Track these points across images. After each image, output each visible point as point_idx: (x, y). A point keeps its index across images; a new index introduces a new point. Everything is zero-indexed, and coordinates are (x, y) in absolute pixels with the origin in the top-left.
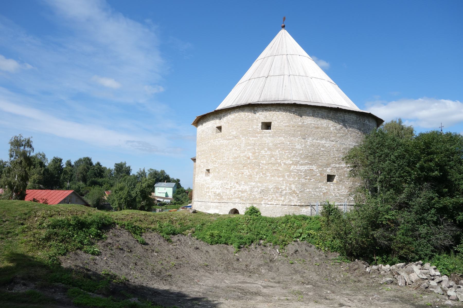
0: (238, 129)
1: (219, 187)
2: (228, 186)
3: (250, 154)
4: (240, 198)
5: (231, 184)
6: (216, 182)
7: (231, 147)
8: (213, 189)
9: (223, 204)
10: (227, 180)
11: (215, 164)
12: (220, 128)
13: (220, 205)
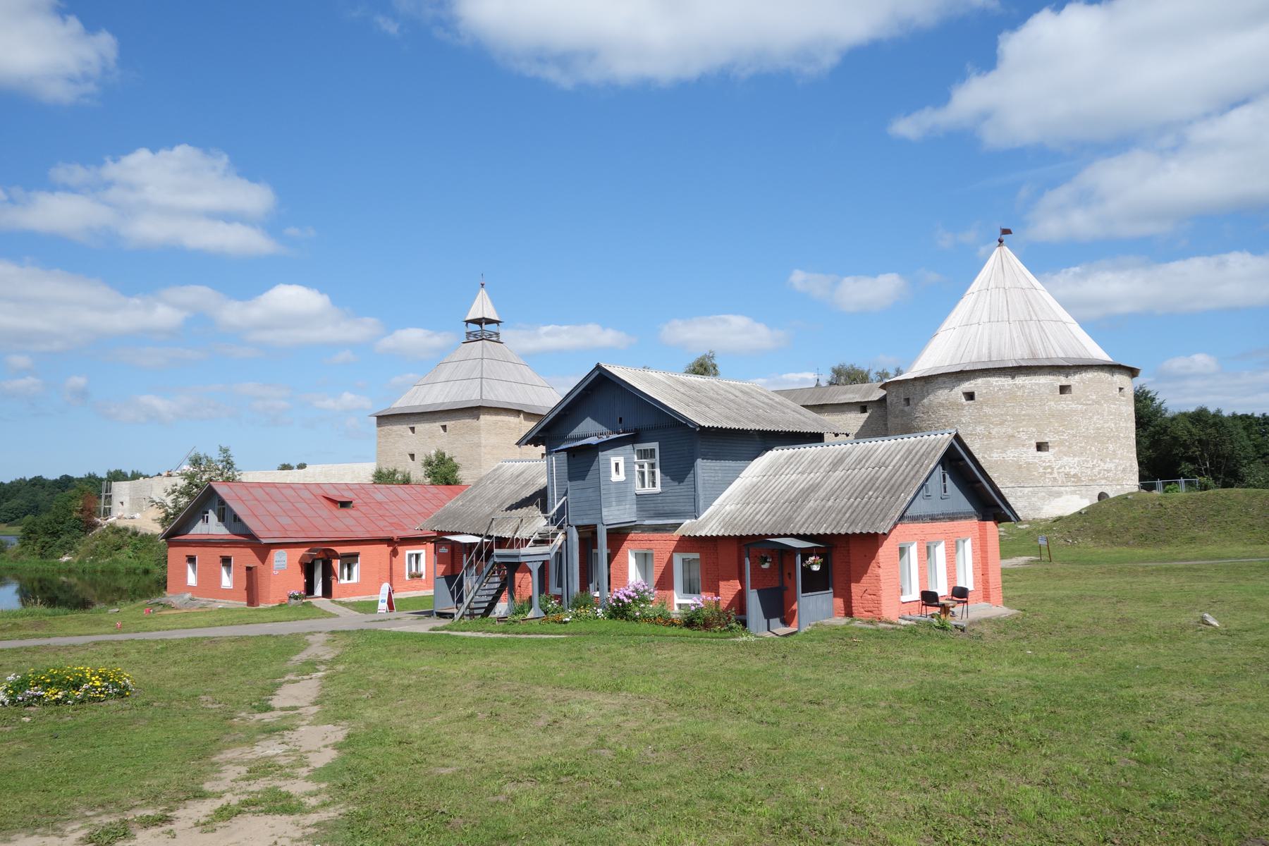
0: (1098, 392)
1: (1075, 465)
3: (1113, 425)
4: (1105, 478)
5: (1092, 462)
9: (1083, 488)
11: (1062, 435)
12: (1064, 389)
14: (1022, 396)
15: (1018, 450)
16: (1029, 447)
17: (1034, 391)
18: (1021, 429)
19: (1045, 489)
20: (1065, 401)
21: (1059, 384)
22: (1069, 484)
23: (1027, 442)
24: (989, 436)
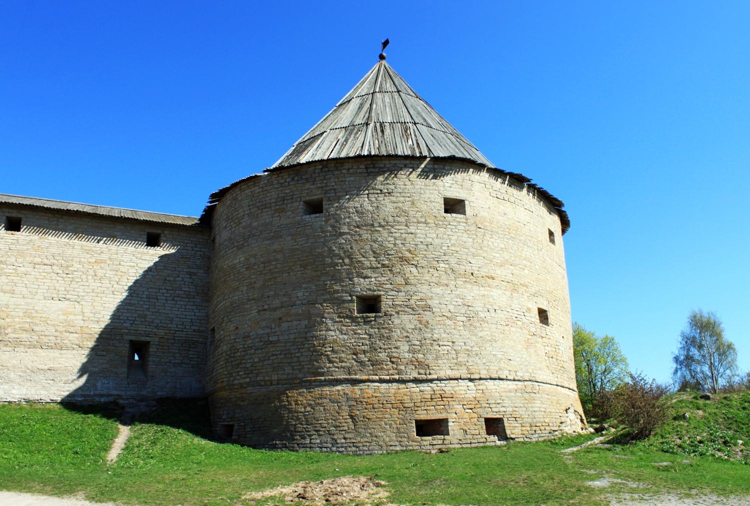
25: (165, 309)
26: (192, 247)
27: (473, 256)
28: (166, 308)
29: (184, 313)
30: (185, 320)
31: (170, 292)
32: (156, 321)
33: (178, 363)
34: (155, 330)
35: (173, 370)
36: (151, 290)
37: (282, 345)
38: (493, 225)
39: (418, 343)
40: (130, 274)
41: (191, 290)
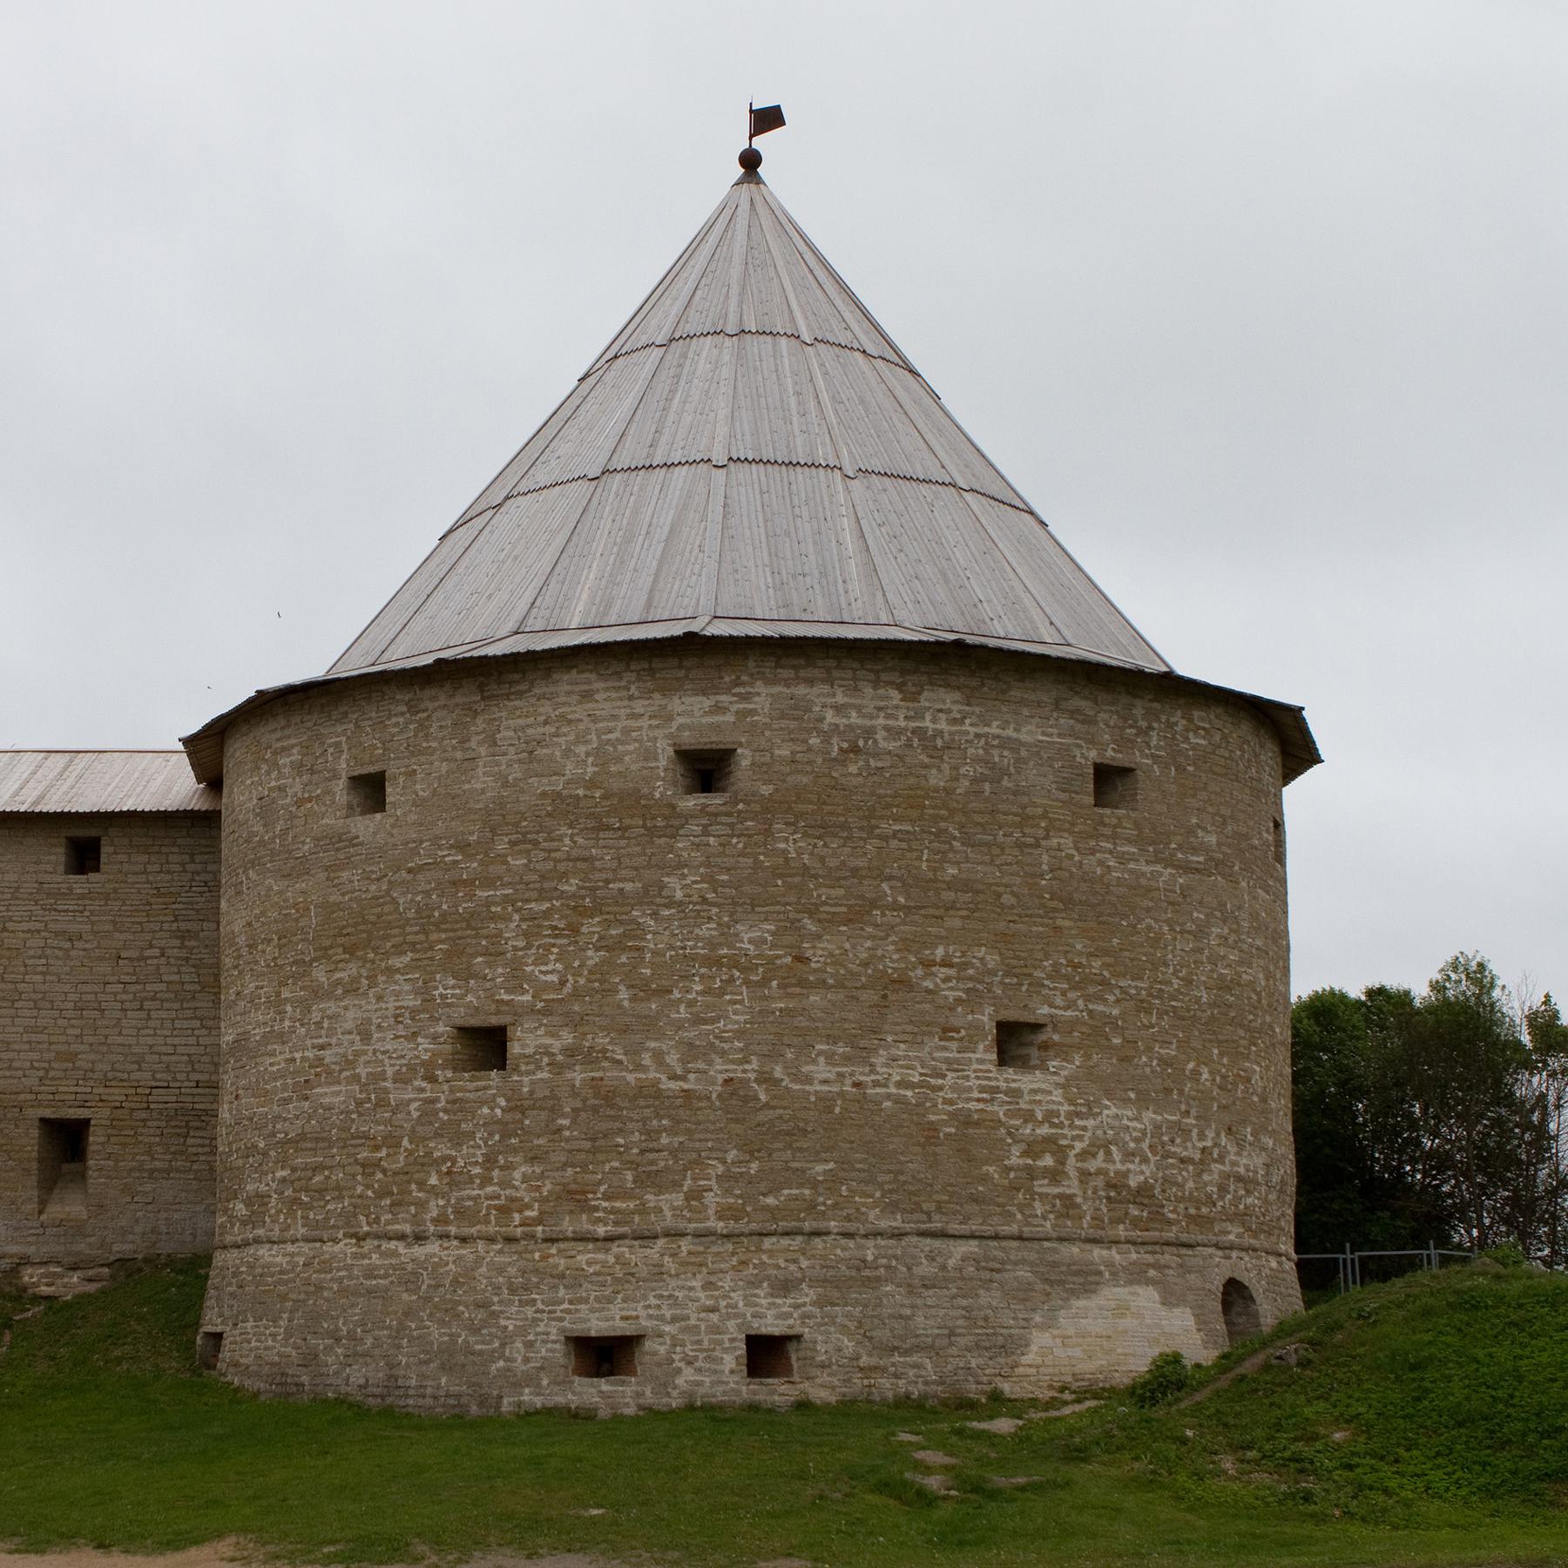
1: (1145, 1146)
2: (1189, 1144)
5: (1202, 1137)
6: (1114, 1110)
7: (1202, 916)
8: (1101, 1155)
9: (1168, 1257)
10: (1183, 1107)
13: (1150, 1258)
14: (949, 792)
15: (924, 1054)
16: (968, 1046)
17: (997, 774)
18: (940, 952)
19: (1030, 1253)
20: (1114, 838)
21: (1093, 754)
22: (1121, 1231)
23: (961, 1018)
24: (798, 976)
25: (120, 1034)
26: (183, 864)
27: (753, 906)
28: (125, 1032)
29: (169, 1041)
30: (173, 1058)
31: (133, 988)
32: (99, 1066)
33: (160, 1170)
34: (101, 1090)
35: (148, 1187)
36: (85, 988)
37: (309, 1145)
38: (827, 808)
39: (587, 1145)
40: (31, 953)
41: (187, 978)
